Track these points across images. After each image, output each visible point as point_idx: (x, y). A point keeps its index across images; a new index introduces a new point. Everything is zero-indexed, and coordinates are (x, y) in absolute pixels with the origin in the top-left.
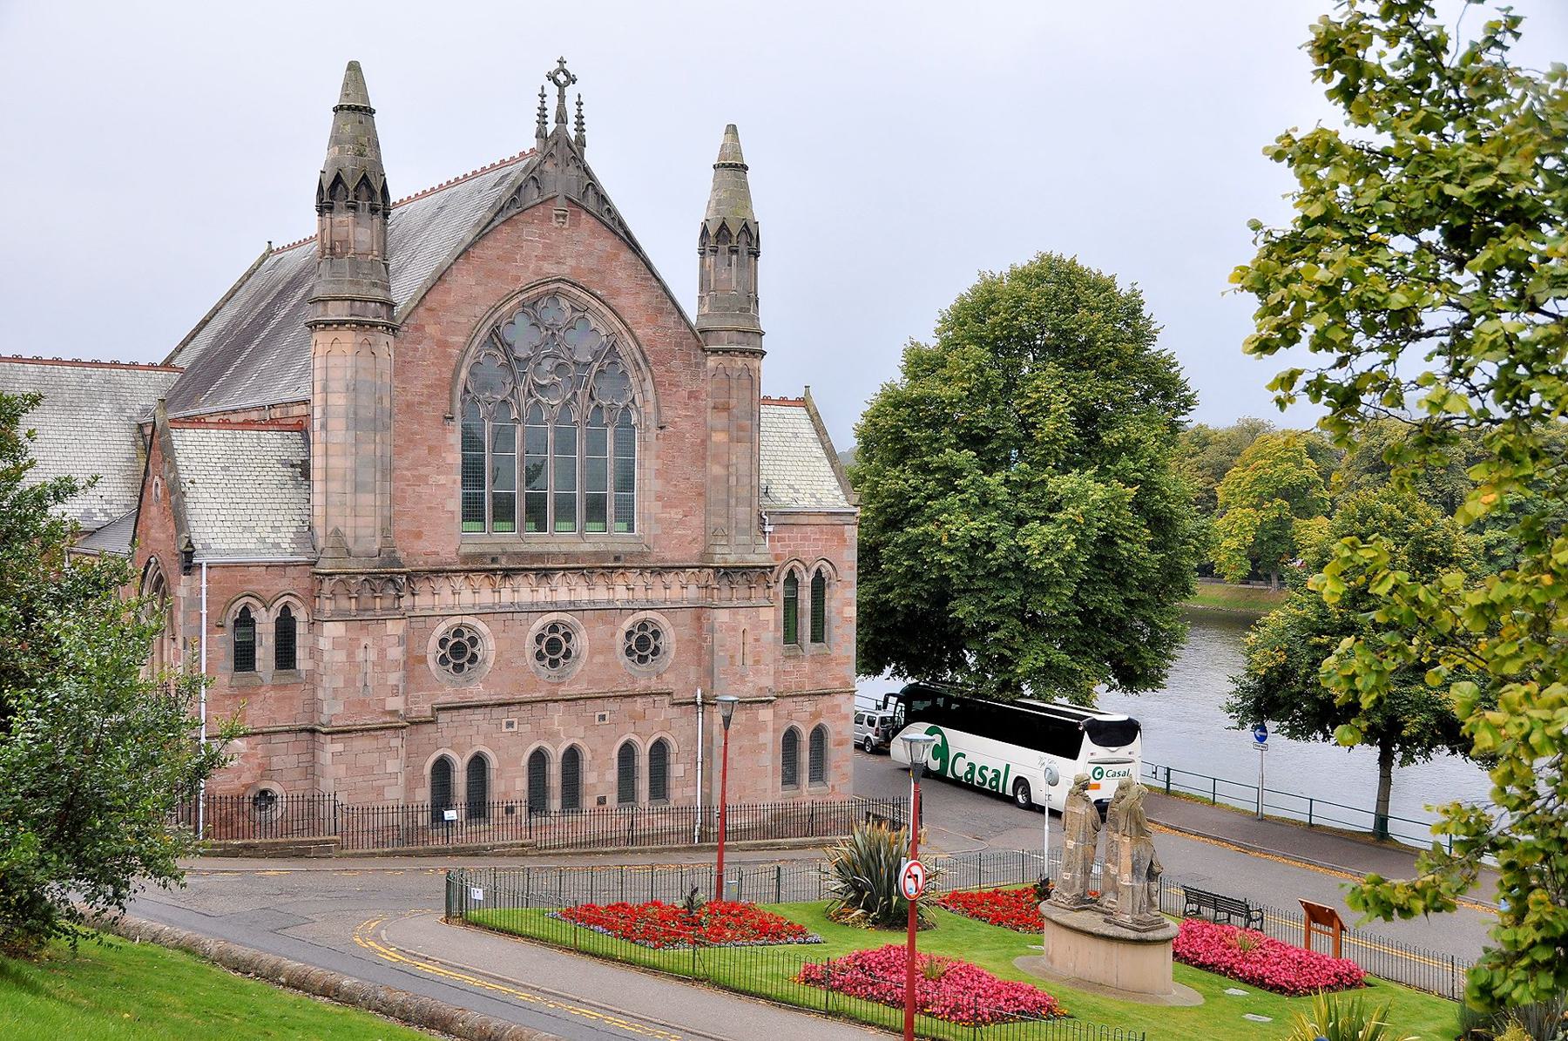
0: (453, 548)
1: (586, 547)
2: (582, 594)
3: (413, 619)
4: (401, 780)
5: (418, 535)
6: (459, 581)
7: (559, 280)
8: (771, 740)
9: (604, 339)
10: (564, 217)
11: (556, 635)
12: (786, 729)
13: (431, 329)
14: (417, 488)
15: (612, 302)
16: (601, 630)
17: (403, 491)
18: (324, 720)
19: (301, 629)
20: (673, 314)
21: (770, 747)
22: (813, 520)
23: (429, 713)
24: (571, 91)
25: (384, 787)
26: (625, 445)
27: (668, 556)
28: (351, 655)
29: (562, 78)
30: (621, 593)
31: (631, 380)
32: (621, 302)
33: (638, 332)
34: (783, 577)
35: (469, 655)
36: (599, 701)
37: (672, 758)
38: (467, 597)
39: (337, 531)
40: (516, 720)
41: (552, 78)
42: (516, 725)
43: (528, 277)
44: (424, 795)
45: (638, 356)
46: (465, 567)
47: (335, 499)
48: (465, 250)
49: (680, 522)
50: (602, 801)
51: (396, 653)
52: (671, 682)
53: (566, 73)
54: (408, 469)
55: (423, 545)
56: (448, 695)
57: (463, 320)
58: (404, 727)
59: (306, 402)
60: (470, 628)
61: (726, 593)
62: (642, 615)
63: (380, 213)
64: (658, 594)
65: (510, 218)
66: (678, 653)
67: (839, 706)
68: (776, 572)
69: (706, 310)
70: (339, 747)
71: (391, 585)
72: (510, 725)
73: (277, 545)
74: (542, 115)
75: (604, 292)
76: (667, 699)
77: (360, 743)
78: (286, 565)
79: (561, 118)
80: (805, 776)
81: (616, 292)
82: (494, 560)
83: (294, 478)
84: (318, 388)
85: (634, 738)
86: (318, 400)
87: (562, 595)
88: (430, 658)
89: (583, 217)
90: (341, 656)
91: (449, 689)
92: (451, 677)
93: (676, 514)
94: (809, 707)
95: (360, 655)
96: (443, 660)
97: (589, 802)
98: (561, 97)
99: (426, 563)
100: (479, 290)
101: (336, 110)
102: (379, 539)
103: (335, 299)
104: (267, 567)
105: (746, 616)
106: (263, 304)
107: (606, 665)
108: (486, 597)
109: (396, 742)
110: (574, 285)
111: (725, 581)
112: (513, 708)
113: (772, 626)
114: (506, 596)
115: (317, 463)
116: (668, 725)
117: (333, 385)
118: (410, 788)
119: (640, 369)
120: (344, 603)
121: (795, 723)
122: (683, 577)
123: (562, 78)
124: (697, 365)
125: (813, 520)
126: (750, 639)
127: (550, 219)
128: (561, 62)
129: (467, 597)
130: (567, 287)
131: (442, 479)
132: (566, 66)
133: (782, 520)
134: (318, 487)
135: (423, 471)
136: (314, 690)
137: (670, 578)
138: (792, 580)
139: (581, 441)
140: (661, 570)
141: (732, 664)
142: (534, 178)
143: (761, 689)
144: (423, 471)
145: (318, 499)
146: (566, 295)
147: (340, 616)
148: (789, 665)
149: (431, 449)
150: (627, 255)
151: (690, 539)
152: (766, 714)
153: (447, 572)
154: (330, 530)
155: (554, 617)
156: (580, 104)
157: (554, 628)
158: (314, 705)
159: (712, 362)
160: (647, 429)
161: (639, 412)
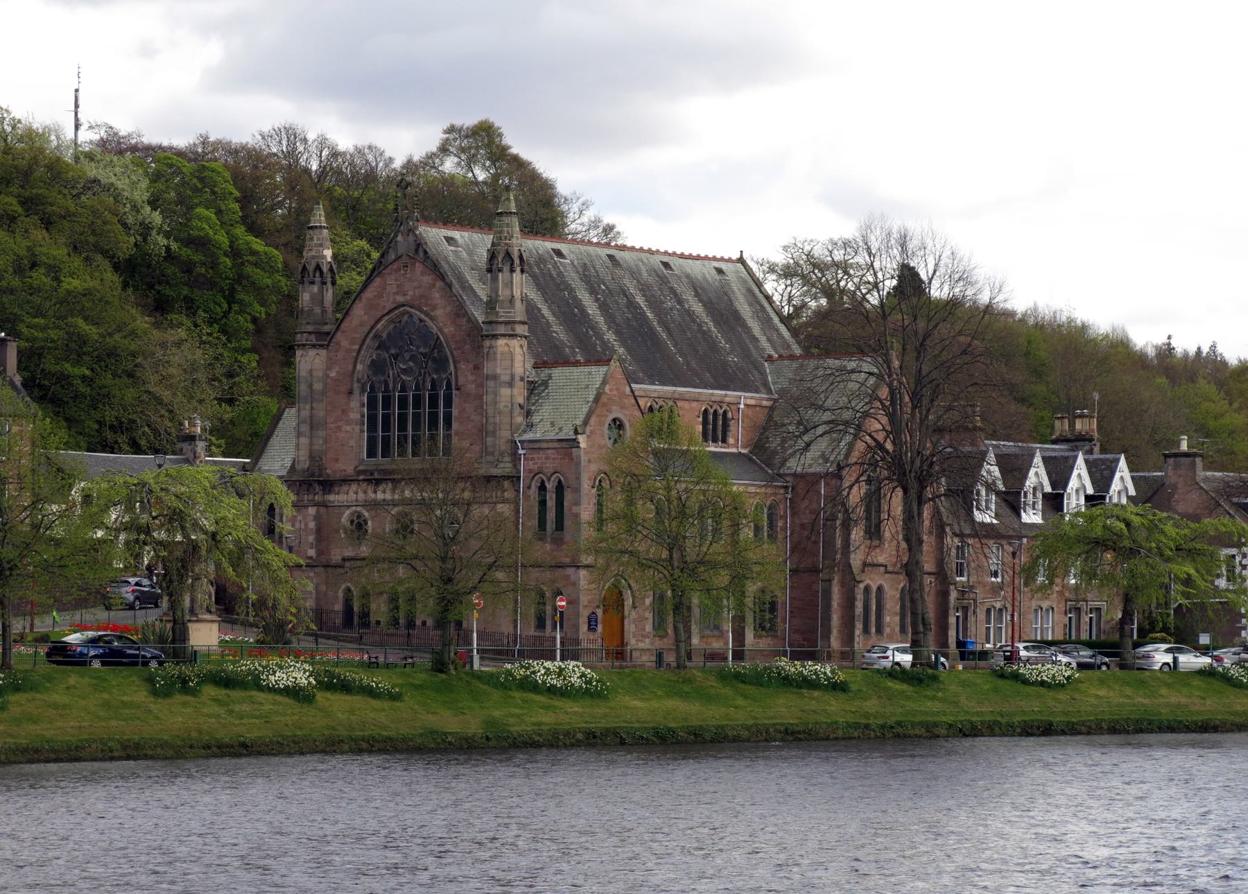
0: (352, 467)
4: (314, 596)
5: (337, 460)
6: (354, 487)
7: (404, 305)
13: (345, 343)
15: (432, 314)
22: (551, 445)
32: (439, 313)
33: (446, 330)
43: (389, 306)
50: (424, 623)
51: (312, 525)
56: (349, 553)
67: (569, 576)
94: (548, 575)
97: (418, 622)
114: (380, 496)
124: (479, 347)
125: (551, 445)
131: (348, 428)
133: (531, 446)
138: (542, 488)
144: (340, 424)
149: (344, 411)
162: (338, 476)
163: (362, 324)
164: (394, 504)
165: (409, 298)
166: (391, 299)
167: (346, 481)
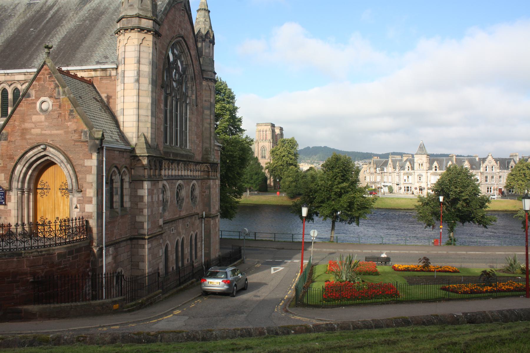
28: (152, 198)
31: (188, 85)
45: (193, 75)
76: (197, 216)
104: (120, 151)
117: (142, 61)
119: (193, 81)
159: (204, 83)
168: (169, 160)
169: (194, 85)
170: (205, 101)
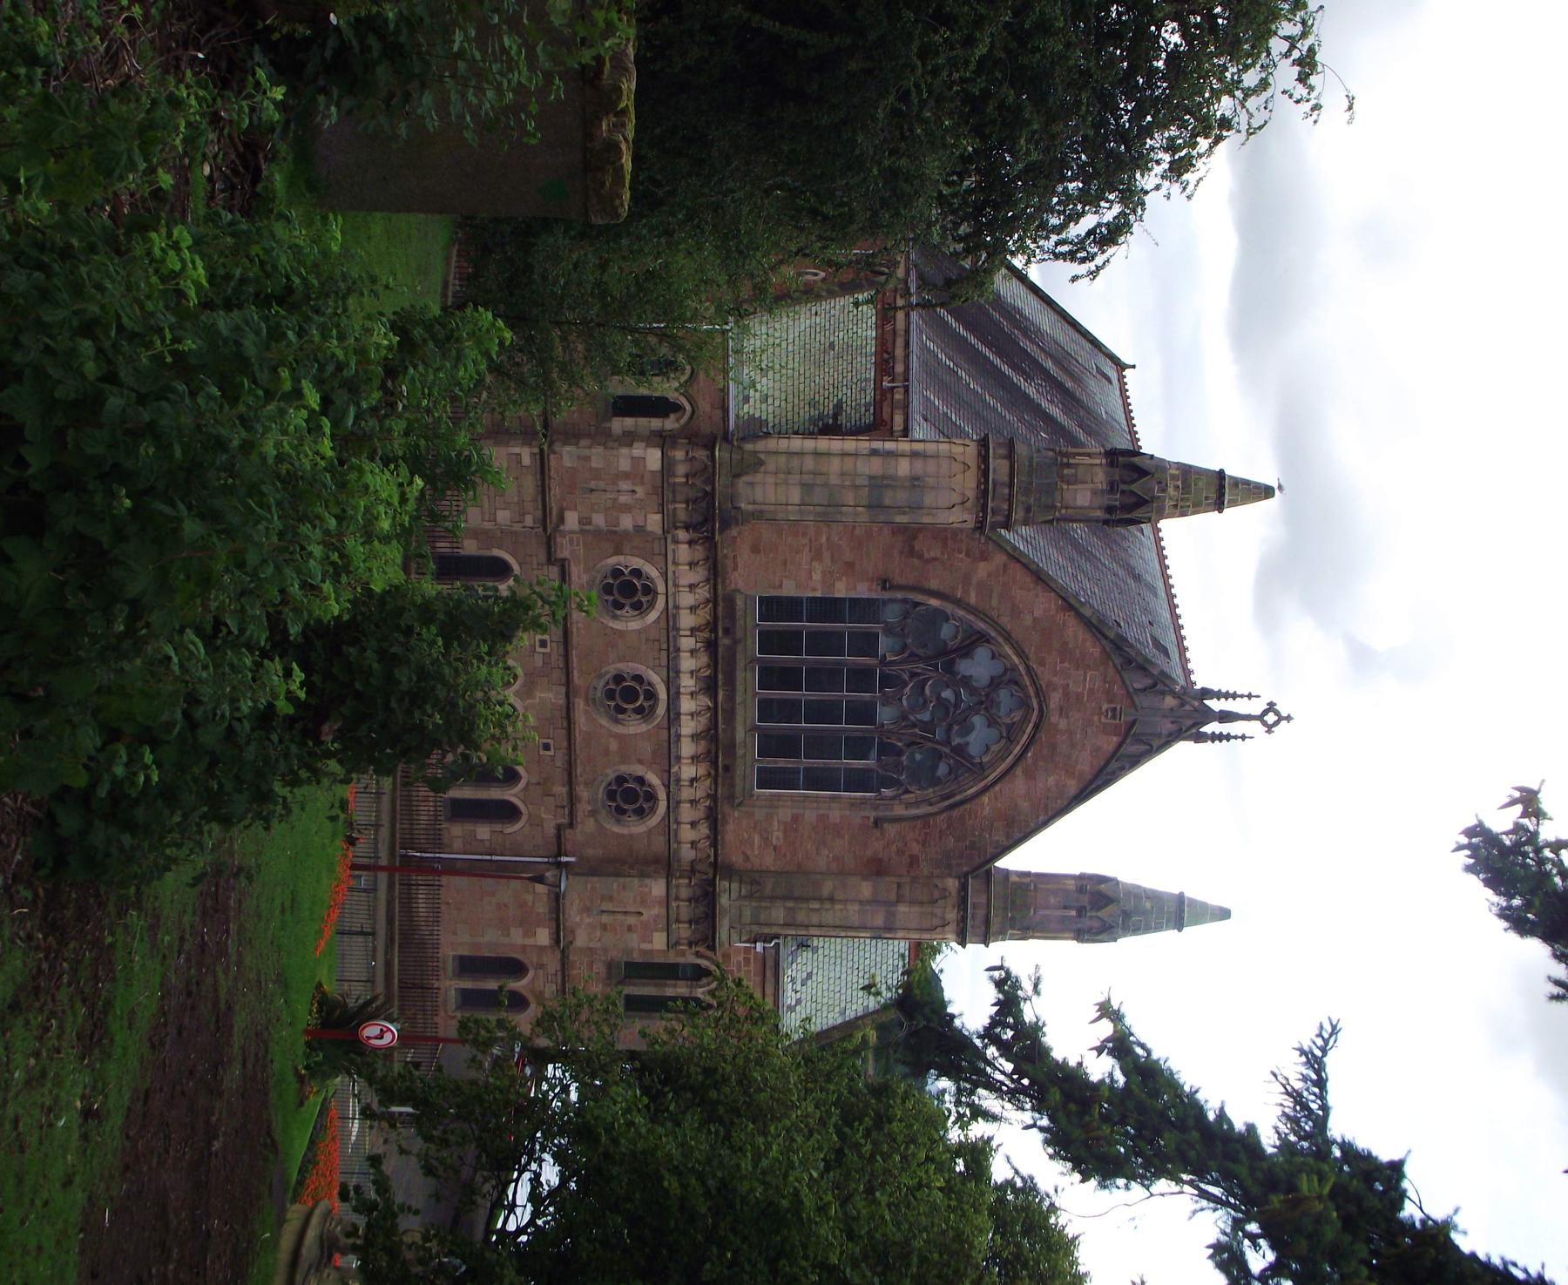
0: (741, 585)
1: (740, 735)
2: (688, 727)
3: (663, 542)
4: (488, 525)
5: (755, 549)
8: (514, 941)
9: (978, 760)
10: (1114, 717)
11: (642, 697)
12: (526, 961)
13: (983, 570)
14: (808, 548)
15: (1019, 771)
16: (647, 748)
17: (804, 534)
18: (557, 447)
19: (655, 423)
20: (1007, 838)
21: (505, 940)
23: (560, 555)
24: (1254, 728)
25: (482, 507)
26: (858, 781)
27: (730, 827)
28: (626, 476)
29: (1271, 717)
30: (688, 771)
32: (1019, 784)
33: (985, 799)
34: (704, 963)
35: (623, 601)
36: (565, 744)
37: (498, 827)
38: (687, 599)
39: (761, 463)
40: (548, 650)
41: (1271, 707)
42: (543, 650)
43: (1045, 676)
44: (470, 548)
45: (958, 798)
46: (720, 599)
47: (795, 462)
48: (1071, 607)
49: (766, 840)
51: (626, 522)
52: (587, 826)
53: (1276, 723)
54: (828, 539)
55: (745, 555)
57: (994, 603)
58: (545, 529)
59: (906, 432)
60: (652, 604)
61: (685, 893)
62: (662, 795)
63: (1108, 516)
64: (686, 813)
65: (1108, 656)
66: (623, 836)
68: (709, 953)
69: (1014, 878)
70: (526, 460)
71: (700, 519)
72: (543, 644)
73: (746, 399)
74: (1227, 696)
75: (1030, 761)
76: (565, 821)
77: (530, 484)
78: (726, 410)
79: (1226, 717)
80: (468, 984)
81: (1030, 776)
82: (727, 631)
83: (821, 417)
84: (918, 447)
85: (522, 784)
86: (904, 446)
87: (687, 705)
88: (621, 558)
89: (1115, 739)
90: (625, 465)
91: (585, 578)
92: (598, 581)
93: (777, 836)
95: (625, 485)
96: (617, 573)
98: (1248, 718)
99: (725, 556)
100: (1028, 620)
101: (1221, 473)
102: (750, 507)
103: (1012, 467)
105: (657, 916)
106: (1049, 364)
107: (606, 752)
108: (687, 620)
109: (529, 520)
110: (1037, 727)
111: (699, 892)
112: (561, 648)
113: (645, 946)
114: (687, 643)
115: (835, 444)
116: (536, 822)
117: (919, 465)
118: (476, 534)
120: (681, 469)
121: (531, 974)
122: (704, 844)
123: (1271, 717)
124: (949, 866)
126: (632, 920)
127: (1110, 701)
128: (1288, 718)
129: (687, 599)
130: (1034, 719)
131: (817, 576)
132: (1284, 723)
133: (770, 963)
134: (809, 444)
135: (826, 555)
136: (589, 436)
137: (704, 829)
138: (699, 974)
139: (857, 730)
140: (714, 819)
141: (603, 899)
142: (1155, 685)
143: (573, 932)
144: (826, 555)
145: (797, 443)
146: (1025, 719)
147: (667, 466)
148: (600, 968)
150: (1072, 787)
151: (748, 853)
152: (543, 937)
153: (715, 579)
154: (762, 456)
155: (662, 695)
156: (1243, 737)
157: (651, 695)
158: (572, 435)
159: (952, 884)
160: (876, 808)
161: (893, 798)
162: (723, 551)
163: (1016, 613)
164: (672, 683)
165: (1054, 719)
166: (1056, 679)
167: (715, 570)
168: (714, 630)
169: (931, 804)
170: (899, 885)
